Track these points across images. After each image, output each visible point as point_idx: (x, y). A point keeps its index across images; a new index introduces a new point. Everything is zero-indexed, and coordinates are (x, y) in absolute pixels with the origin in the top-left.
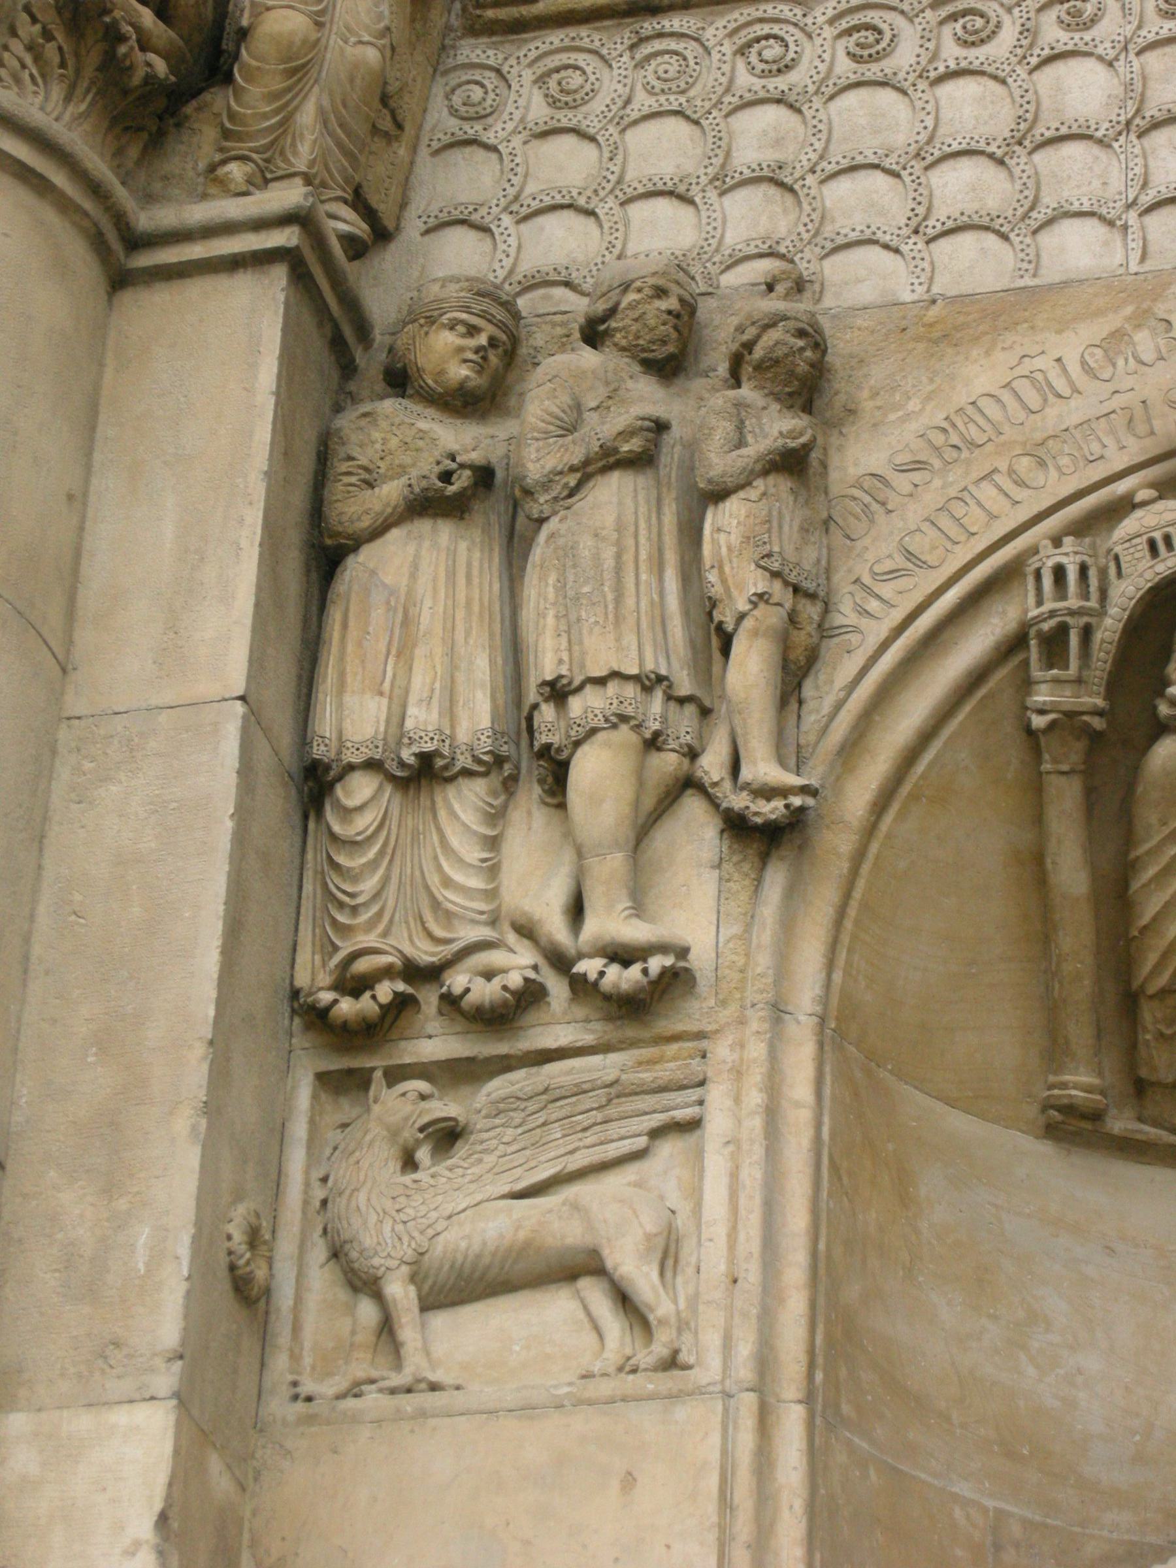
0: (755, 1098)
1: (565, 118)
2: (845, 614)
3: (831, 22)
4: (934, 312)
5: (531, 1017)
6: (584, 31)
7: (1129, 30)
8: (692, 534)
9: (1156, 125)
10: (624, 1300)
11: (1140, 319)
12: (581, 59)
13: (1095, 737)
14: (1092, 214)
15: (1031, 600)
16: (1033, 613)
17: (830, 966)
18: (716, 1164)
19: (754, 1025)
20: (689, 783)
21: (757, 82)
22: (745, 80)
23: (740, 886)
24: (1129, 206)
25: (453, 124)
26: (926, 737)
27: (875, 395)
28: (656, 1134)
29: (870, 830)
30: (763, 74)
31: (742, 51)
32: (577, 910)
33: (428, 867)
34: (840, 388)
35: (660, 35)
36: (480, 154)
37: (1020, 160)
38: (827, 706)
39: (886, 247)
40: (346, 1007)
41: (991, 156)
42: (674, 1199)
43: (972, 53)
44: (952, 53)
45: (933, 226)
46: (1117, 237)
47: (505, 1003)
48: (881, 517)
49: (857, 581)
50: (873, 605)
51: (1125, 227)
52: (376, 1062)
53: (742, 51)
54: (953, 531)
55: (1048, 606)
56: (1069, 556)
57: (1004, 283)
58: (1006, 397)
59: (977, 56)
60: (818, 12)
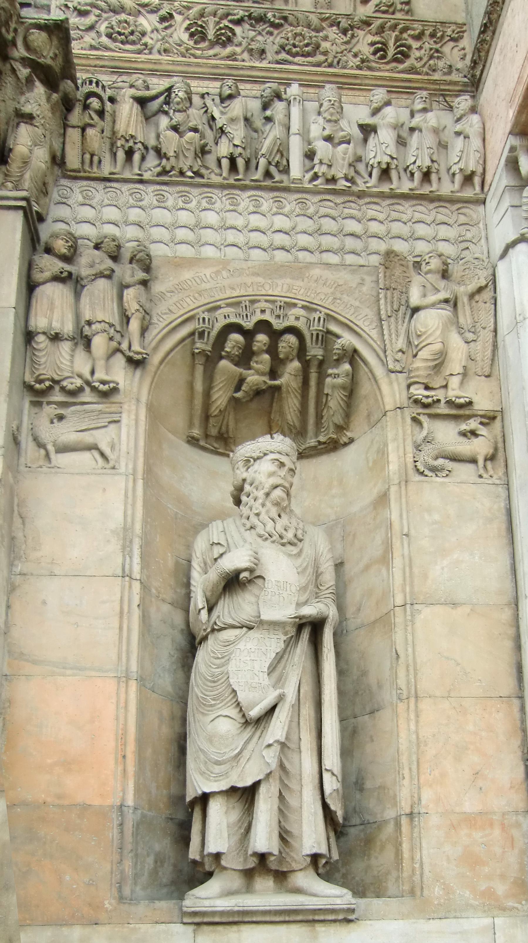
0: (133, 417)
1: (88, 202)
2: (155, 320)
3: (152, 192)
4: (176, 260)
5: (81, 395)
6: (92, 183)
7: (223, 207)
8: (120, 297)
9: (228, 228)
10: (102, 455)
11: (224, 268)
12: (91, 189)
13: (207, 357)
14: (213, 245)
15: (197, 324)
16: (197, 327)
17: (149, 394)
18: (124, 430)
19: (133, 402)
20: (118, 350)
21: (135, 203)
22: (131, 201)
23: (130, 374)
24: (222, 244)
25: (59, 198)
26: (172, 350)
27: (162, 275)
28: (110, 422)
29: (158, 368)
30: (136, 201)
31: (131, 195)
32: (93, 373)
33: (57, 359)
34: (154, 272)
35: (111, 187)
36: (66, 207)
37: (196, 230)
38: (151, 338)
39: (165, 244)
40: (38, 386)
41: (190, 228)
42: (114, 436)
43: (186, 205)
44: (181, 204)
45: (176, 241)
46: (218, 252)
47: (76, 390)
48: (163, 301)
49: (158, 314)
50: (161, 319)
51: (220, 249)
52: (45, 400)
53: (131, 195)
54: (180, 307)
55: (201, 325)
56: (206, 316)
57: (193, 256)
58: (192, 280)
59: (187, 206)
60: (149, 189)
